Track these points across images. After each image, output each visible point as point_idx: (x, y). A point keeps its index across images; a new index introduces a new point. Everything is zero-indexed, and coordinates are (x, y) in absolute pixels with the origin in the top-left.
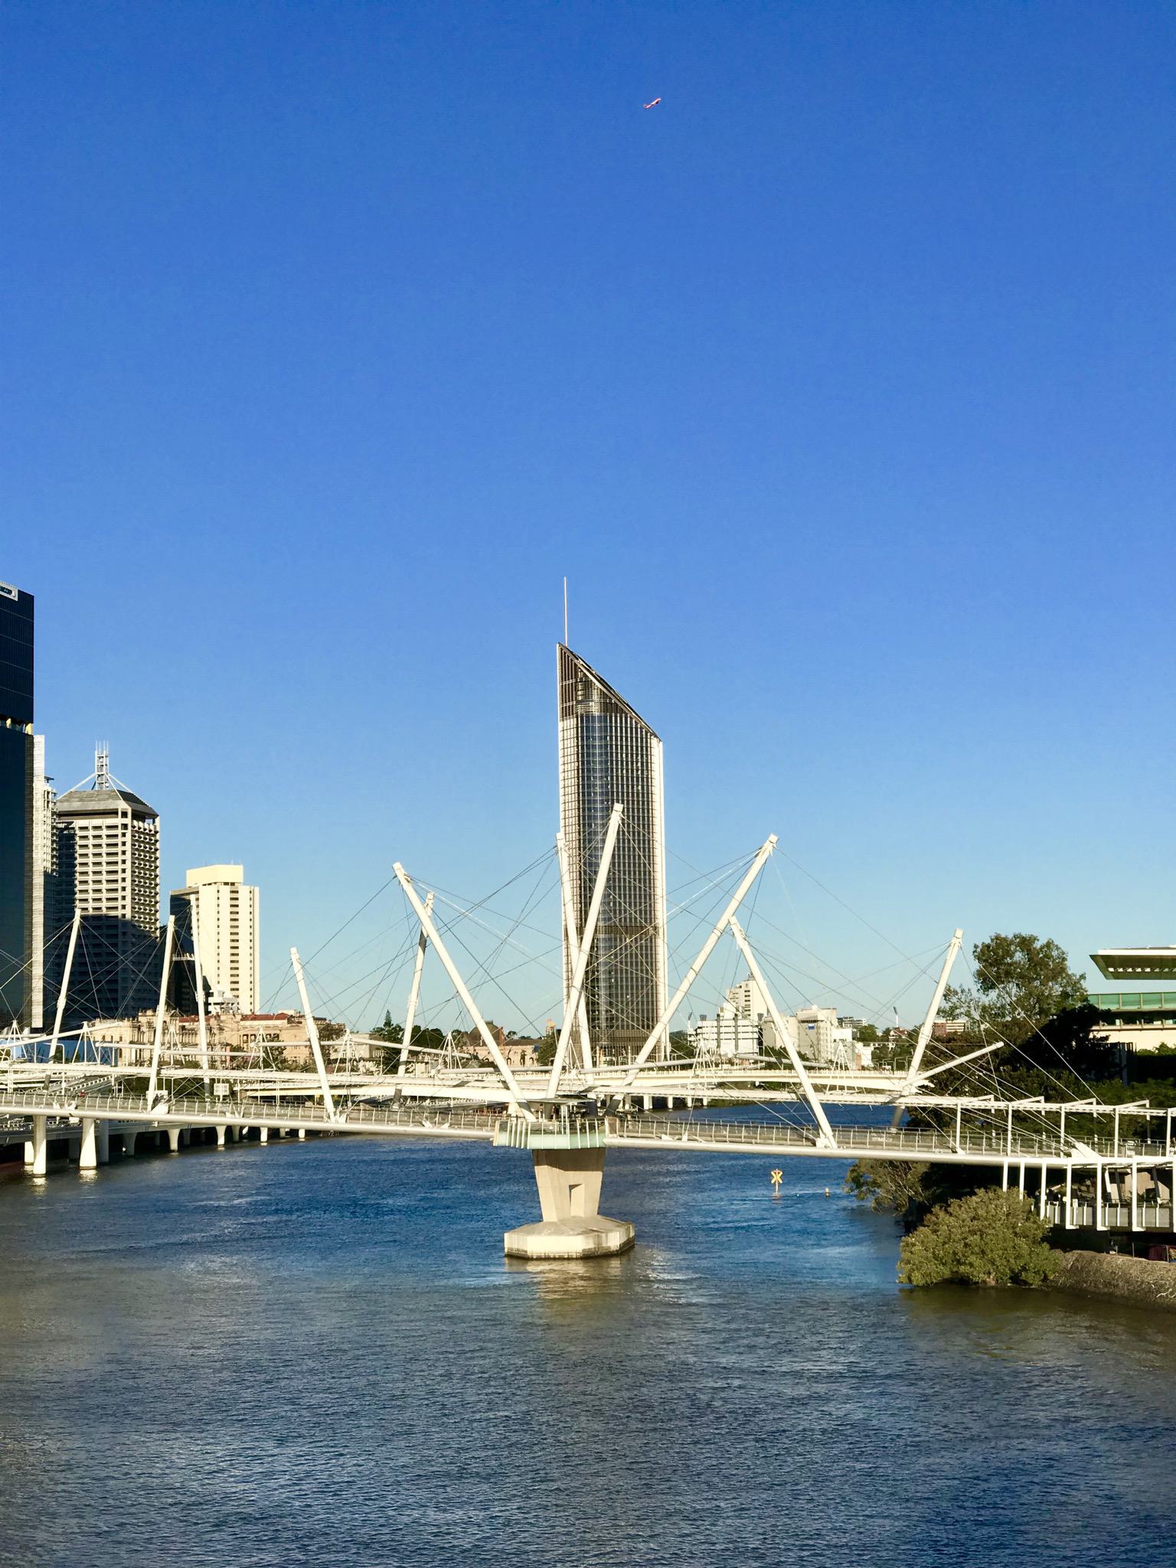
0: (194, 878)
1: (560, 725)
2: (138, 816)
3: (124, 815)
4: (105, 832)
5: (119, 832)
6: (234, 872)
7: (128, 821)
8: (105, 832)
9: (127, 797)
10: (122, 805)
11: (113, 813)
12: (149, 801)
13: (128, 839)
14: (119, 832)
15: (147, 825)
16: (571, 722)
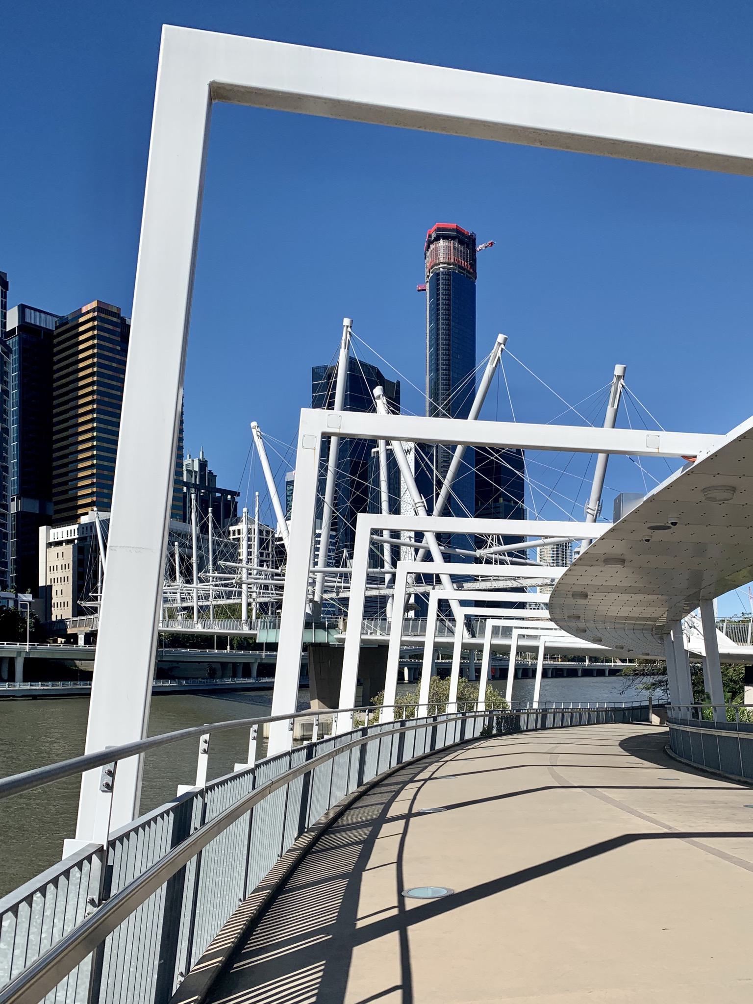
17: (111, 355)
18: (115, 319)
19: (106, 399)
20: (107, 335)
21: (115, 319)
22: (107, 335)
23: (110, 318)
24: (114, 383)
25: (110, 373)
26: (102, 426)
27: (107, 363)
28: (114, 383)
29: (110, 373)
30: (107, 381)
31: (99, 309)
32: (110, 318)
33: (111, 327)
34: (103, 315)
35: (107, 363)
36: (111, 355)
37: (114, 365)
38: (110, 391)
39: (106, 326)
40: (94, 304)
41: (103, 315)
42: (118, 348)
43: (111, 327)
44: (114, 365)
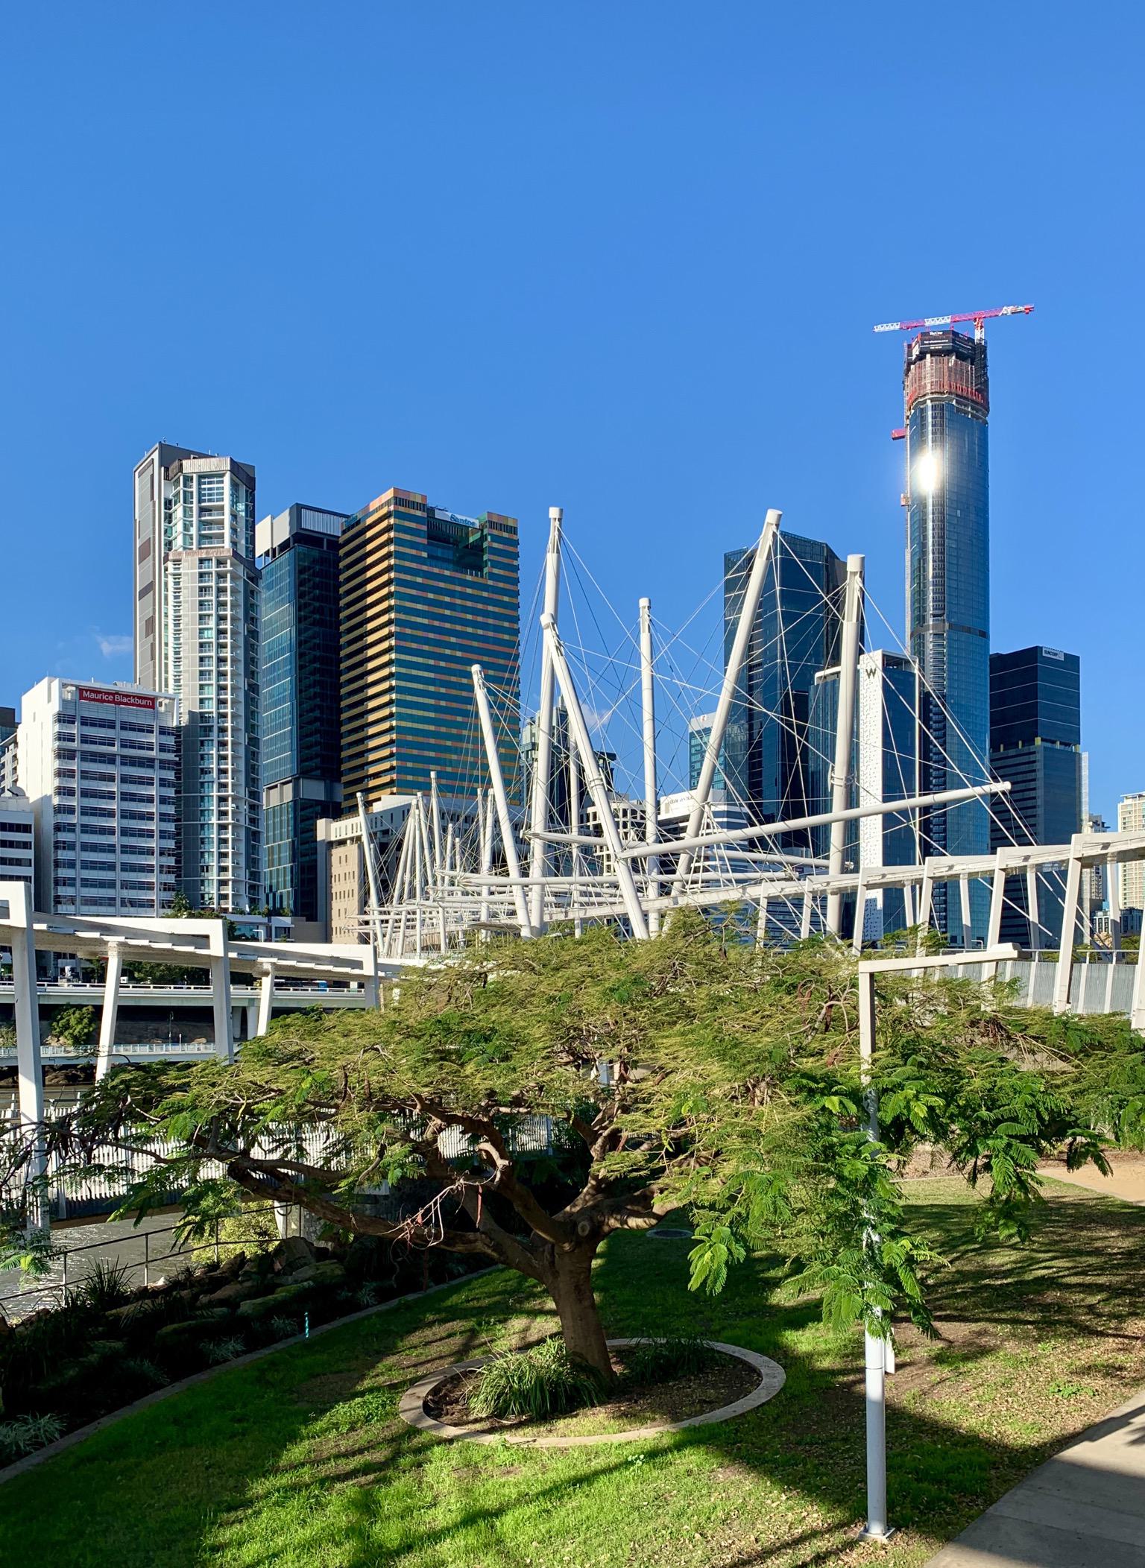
17: (414, 565)
18: (419, 513)
19: (408, 631)
20: (408, 537)
21: (419, 513)
22: (408, 537)
23: (412, 512)
24: (419, 607)
25: (414, 592)
26: (403, 670)
27: (408, 578)
28: (419, 607)
29: (414, 592)
30: (408, 604)
31: (398, 500)
32: (412, 512)
33: (413, 525)
34: (401, 509)
35: (408, 578)
36: (414, 565)
37: (419, 580)
38: (413, 619)
39: (407, 524)
40: (389, 494)
41: (401, 509)
42: (425, 555)
43: (413, 525)
44: (419, 580)
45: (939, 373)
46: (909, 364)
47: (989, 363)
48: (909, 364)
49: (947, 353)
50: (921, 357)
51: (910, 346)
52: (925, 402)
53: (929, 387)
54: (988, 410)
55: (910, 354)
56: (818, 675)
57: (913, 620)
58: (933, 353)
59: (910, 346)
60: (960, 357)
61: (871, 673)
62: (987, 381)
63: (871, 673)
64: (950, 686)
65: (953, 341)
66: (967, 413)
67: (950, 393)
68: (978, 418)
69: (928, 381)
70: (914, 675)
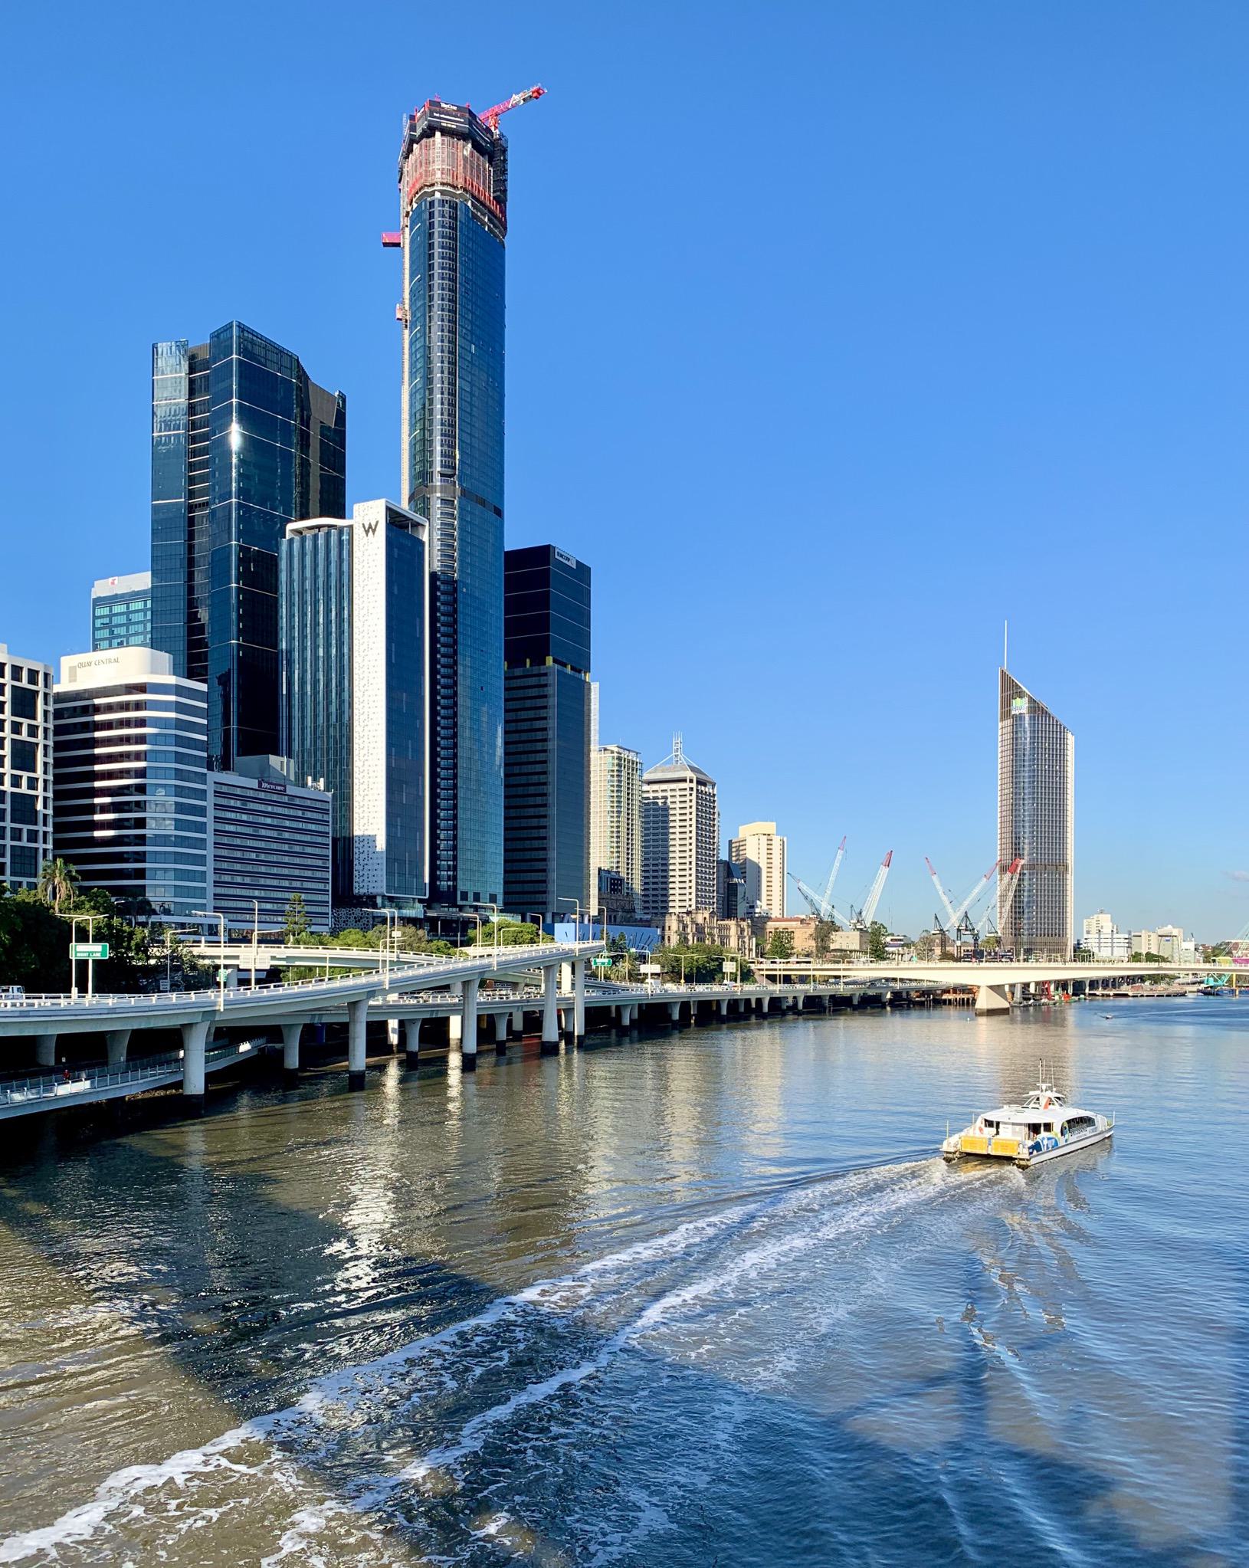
0: (745, 831)
1: (1000, 725)
2: (699, 782)
3: (691, 781)
4: (678, 793)
5: (687, 792)
6: (770, 827)
7: (694, 785)
8: (678, 793)
9: (693, 769)
10: (689, 774)
11: (684, 780)
12: (711, 776)
13: (694, 797)
14: (687, 792)
15: (708, 789)
16: (1009, 722)
45: (453, 157)
46: (413, 141)
47: (510, 166)
48: (413, 141)
49: (463, 136)
50: (429, 133)
51: (412, 118)
52: (433, 194)
53: (439, 174)
54: (505, 228)
55: (413, 128)
56: (290, 526)
57: (413, 477)
58: (445, 132)
59: (412, 118)
60: (477, 146)
61: (370, 529)
62: (505, 191)
63: (370, 529)
64: (461, 571)
65: (470, 124)
66: (483, 224)
67: (465, 190)
68: (496, 236)
69: (438, 165)
70: (422, 544)
